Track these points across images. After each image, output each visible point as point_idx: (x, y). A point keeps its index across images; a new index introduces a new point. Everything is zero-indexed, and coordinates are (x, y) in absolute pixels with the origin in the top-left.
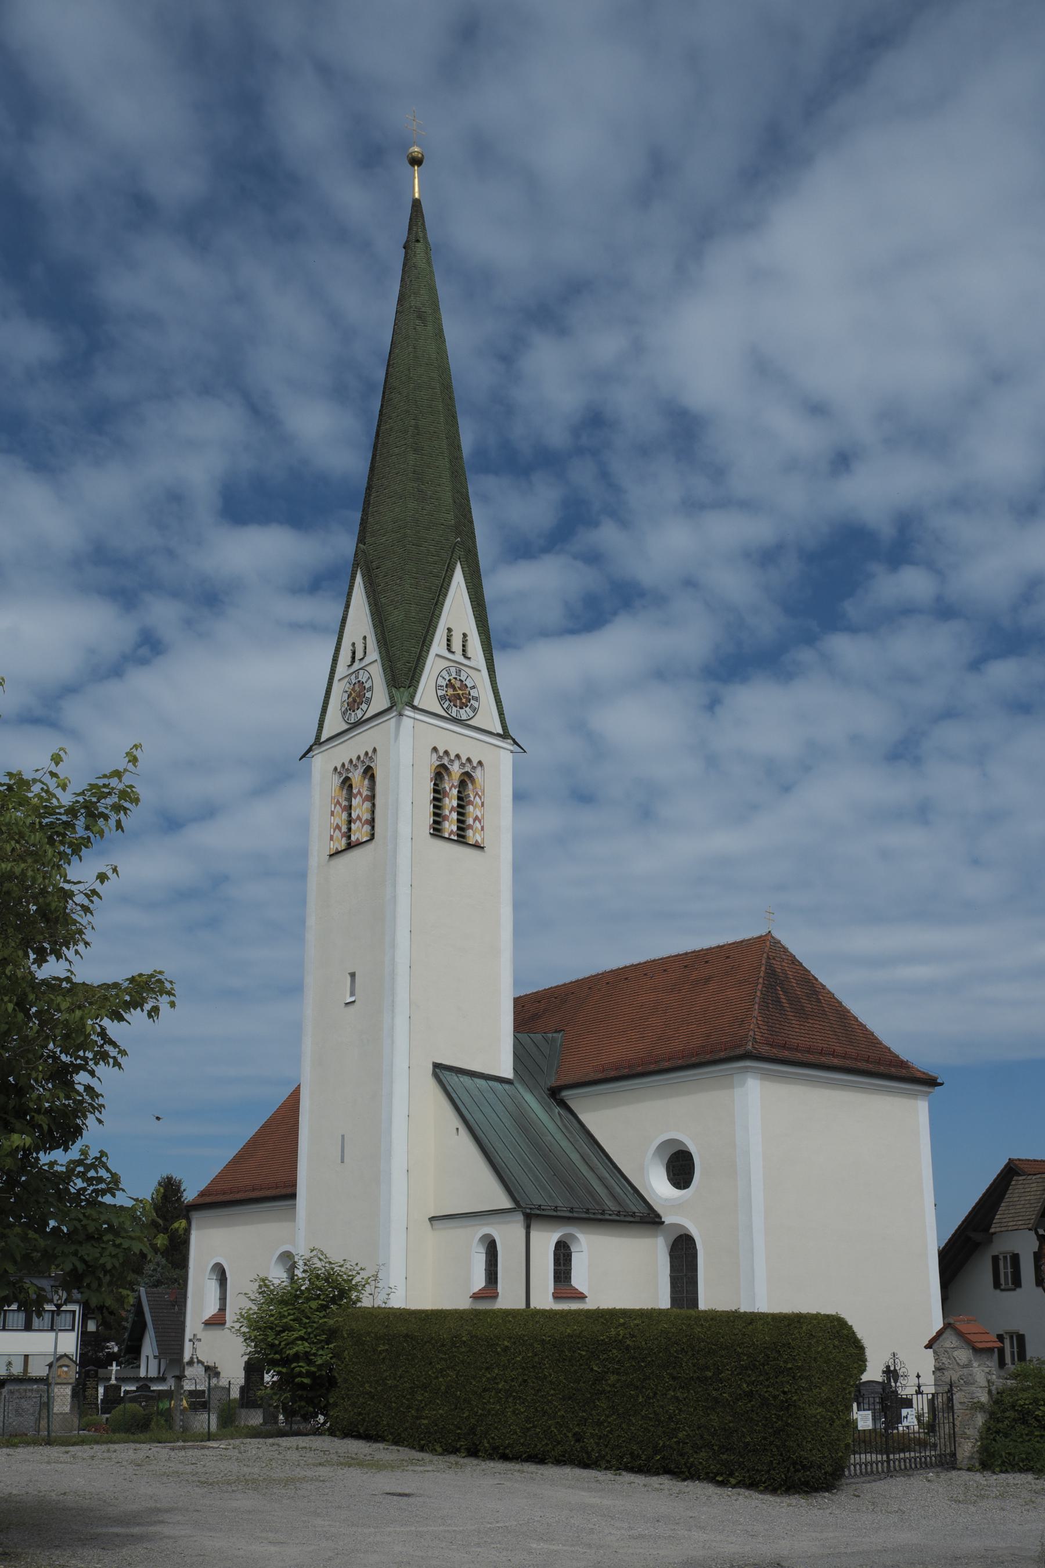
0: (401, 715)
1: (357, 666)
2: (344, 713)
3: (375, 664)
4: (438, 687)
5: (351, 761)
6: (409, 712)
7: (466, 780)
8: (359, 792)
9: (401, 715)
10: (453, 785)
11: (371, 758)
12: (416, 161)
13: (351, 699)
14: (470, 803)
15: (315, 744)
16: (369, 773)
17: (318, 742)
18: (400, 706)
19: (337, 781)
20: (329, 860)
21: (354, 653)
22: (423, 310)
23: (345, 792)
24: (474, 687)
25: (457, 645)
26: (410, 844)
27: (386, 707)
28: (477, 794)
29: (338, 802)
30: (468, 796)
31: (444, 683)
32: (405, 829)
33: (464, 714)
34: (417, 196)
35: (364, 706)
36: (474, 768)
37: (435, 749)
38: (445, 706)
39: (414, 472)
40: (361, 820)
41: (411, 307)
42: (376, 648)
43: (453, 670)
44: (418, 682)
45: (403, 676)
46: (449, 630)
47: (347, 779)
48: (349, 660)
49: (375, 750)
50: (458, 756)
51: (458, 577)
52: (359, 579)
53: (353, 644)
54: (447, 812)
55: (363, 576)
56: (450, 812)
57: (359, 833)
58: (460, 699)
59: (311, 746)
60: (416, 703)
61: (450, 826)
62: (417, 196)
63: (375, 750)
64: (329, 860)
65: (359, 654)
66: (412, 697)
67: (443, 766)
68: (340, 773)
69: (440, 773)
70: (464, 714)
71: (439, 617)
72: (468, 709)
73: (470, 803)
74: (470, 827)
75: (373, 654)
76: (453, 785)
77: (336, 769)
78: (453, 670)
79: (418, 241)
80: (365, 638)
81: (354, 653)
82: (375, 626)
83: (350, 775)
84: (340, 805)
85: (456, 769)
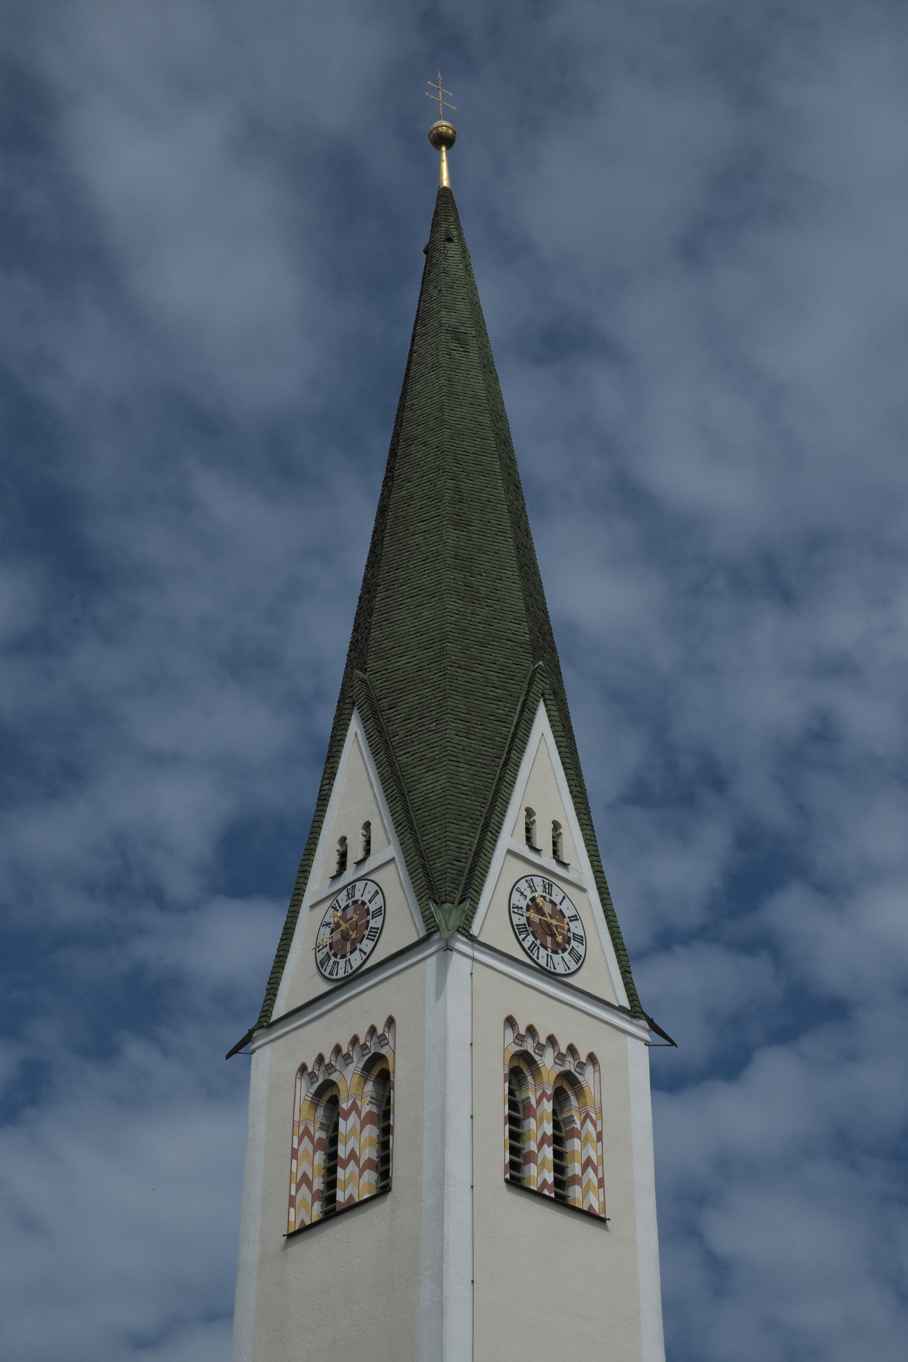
0: (448, 948)
1: (349, 875)
2: (320, 964)
3: (392, 867)
4: (512, 909)
5: (337, 1049)
6: (461, 944)
7: (567, 1087)
8: (354, 1107)
9: (448, 948)
10: (544, 1094)
11: (382, 1037)
12: (442, 140)
13: (337, 936)
14: (574, 1133)
15: (259, 1026)
16: (379, 1071)
17: (265, 1023)
18: (445, 935)
19: (304, 1091)
20: (286, 1246)
21: (343, 856)
22: (462, 329)
23: (320, 1112)
24: (575, 918)
25: (543, 839)
26: (470, 1196)
27: (415, 938)
28: (588, 1116)
29: (306, 1132)
30: (571, 1119)
31: (523, 904)
32: (458, 1168)
33: (560, 963)
34: (445, 183)
35: (367, 945)
36: (581, 1065)
37: (510, 1022)
38: (526, 944)
39: (457, 556)
40: (357, 1162)
41: (441, 325)
42: (392, 835)
43: (538, 882)
44: (479, 893)
45: (447, 880)
46: (530, 813)
47: (329, 1084)
48: (334, 868)
49: (391, 1022)
50: (552, 1040)
51: (542, 725)
52: (355, 727)
53: (343, 840)
54: (533, 1146)
55: (364, 720)
56: (540, 1146)
57: (354, 1183)
58: (553, 936)
59: (251, 1032)
60: (475, 931)
61: (540, 1174)
62: (445, 183)
63: (391, 1022)
64: (286, 1246)
65: (355, 852)
66: (469, 918)
67: (524, 1056)
68: (313, 1076)
69: (520, 1069)
70: (560, 963)
71: (512, 785)
72: (566, 955)
73: (574, 1133)
74: (575, 1180)
75: (386, 847)
76: (544, 1094)
77: (303, 1068)
78: (538, 882)
79: (450, 240)
80: (367, 826)
81: (343, 856)
82: (390, 799)
83: (334, 1077)
84: (311, 1138)
85: (547, 1062)
